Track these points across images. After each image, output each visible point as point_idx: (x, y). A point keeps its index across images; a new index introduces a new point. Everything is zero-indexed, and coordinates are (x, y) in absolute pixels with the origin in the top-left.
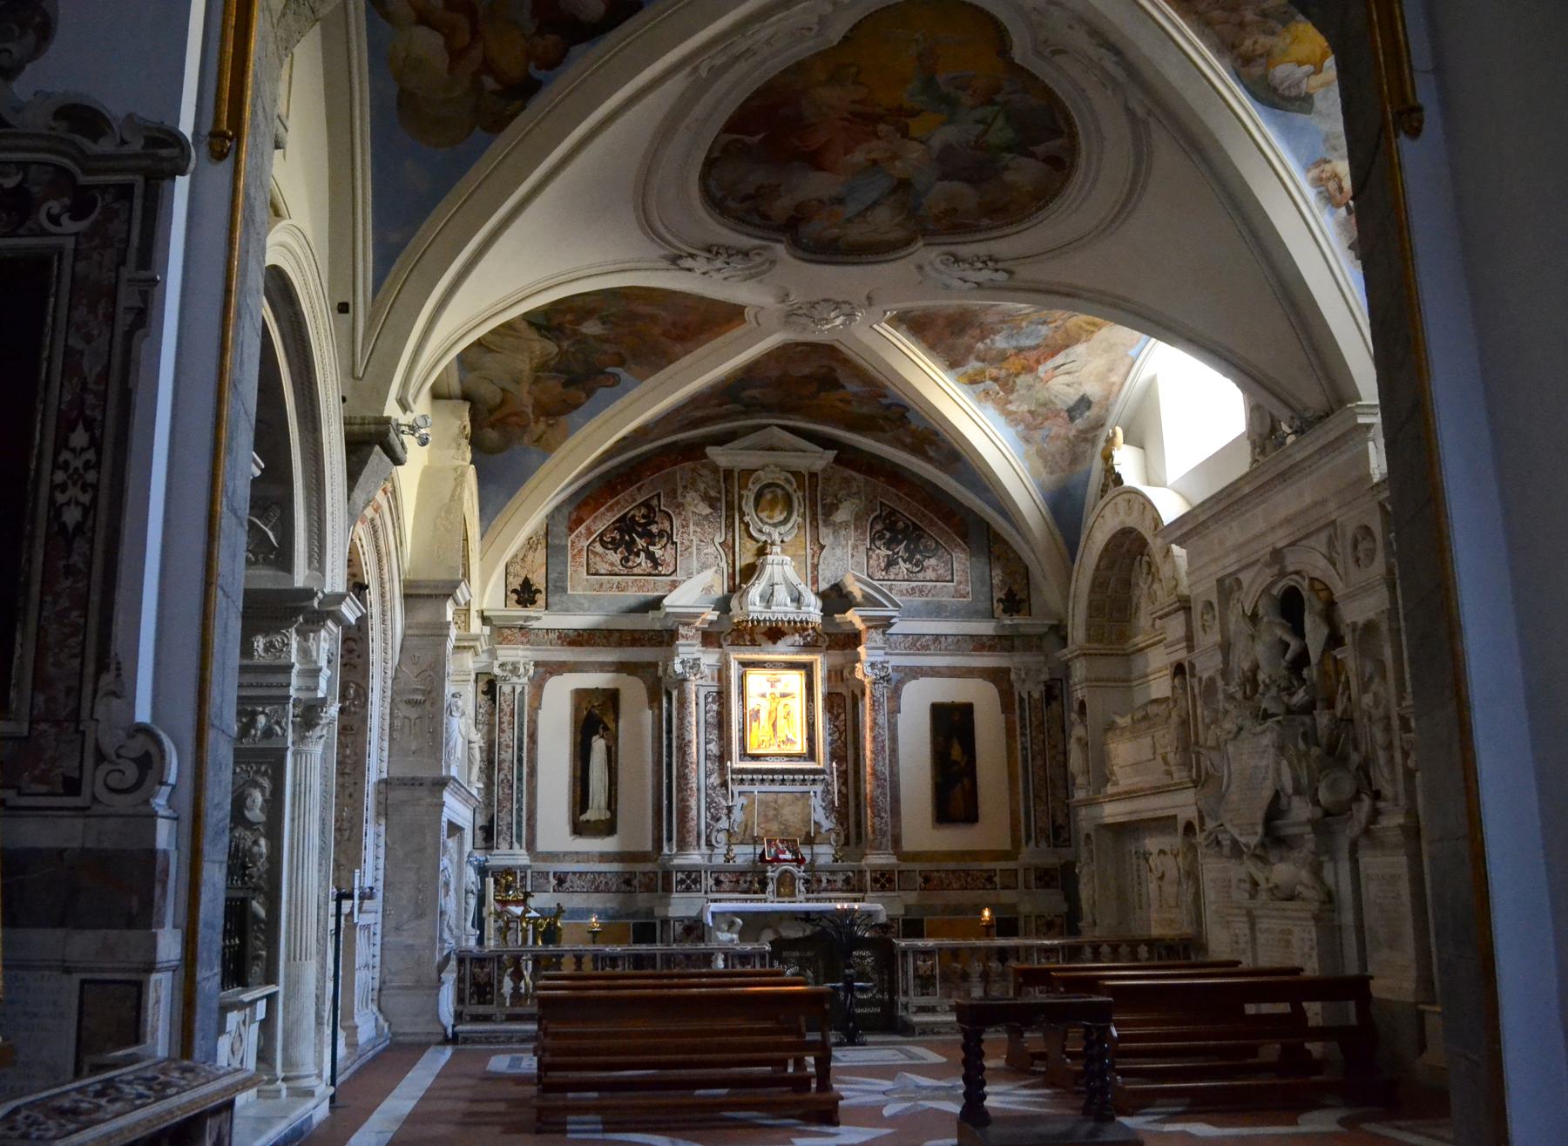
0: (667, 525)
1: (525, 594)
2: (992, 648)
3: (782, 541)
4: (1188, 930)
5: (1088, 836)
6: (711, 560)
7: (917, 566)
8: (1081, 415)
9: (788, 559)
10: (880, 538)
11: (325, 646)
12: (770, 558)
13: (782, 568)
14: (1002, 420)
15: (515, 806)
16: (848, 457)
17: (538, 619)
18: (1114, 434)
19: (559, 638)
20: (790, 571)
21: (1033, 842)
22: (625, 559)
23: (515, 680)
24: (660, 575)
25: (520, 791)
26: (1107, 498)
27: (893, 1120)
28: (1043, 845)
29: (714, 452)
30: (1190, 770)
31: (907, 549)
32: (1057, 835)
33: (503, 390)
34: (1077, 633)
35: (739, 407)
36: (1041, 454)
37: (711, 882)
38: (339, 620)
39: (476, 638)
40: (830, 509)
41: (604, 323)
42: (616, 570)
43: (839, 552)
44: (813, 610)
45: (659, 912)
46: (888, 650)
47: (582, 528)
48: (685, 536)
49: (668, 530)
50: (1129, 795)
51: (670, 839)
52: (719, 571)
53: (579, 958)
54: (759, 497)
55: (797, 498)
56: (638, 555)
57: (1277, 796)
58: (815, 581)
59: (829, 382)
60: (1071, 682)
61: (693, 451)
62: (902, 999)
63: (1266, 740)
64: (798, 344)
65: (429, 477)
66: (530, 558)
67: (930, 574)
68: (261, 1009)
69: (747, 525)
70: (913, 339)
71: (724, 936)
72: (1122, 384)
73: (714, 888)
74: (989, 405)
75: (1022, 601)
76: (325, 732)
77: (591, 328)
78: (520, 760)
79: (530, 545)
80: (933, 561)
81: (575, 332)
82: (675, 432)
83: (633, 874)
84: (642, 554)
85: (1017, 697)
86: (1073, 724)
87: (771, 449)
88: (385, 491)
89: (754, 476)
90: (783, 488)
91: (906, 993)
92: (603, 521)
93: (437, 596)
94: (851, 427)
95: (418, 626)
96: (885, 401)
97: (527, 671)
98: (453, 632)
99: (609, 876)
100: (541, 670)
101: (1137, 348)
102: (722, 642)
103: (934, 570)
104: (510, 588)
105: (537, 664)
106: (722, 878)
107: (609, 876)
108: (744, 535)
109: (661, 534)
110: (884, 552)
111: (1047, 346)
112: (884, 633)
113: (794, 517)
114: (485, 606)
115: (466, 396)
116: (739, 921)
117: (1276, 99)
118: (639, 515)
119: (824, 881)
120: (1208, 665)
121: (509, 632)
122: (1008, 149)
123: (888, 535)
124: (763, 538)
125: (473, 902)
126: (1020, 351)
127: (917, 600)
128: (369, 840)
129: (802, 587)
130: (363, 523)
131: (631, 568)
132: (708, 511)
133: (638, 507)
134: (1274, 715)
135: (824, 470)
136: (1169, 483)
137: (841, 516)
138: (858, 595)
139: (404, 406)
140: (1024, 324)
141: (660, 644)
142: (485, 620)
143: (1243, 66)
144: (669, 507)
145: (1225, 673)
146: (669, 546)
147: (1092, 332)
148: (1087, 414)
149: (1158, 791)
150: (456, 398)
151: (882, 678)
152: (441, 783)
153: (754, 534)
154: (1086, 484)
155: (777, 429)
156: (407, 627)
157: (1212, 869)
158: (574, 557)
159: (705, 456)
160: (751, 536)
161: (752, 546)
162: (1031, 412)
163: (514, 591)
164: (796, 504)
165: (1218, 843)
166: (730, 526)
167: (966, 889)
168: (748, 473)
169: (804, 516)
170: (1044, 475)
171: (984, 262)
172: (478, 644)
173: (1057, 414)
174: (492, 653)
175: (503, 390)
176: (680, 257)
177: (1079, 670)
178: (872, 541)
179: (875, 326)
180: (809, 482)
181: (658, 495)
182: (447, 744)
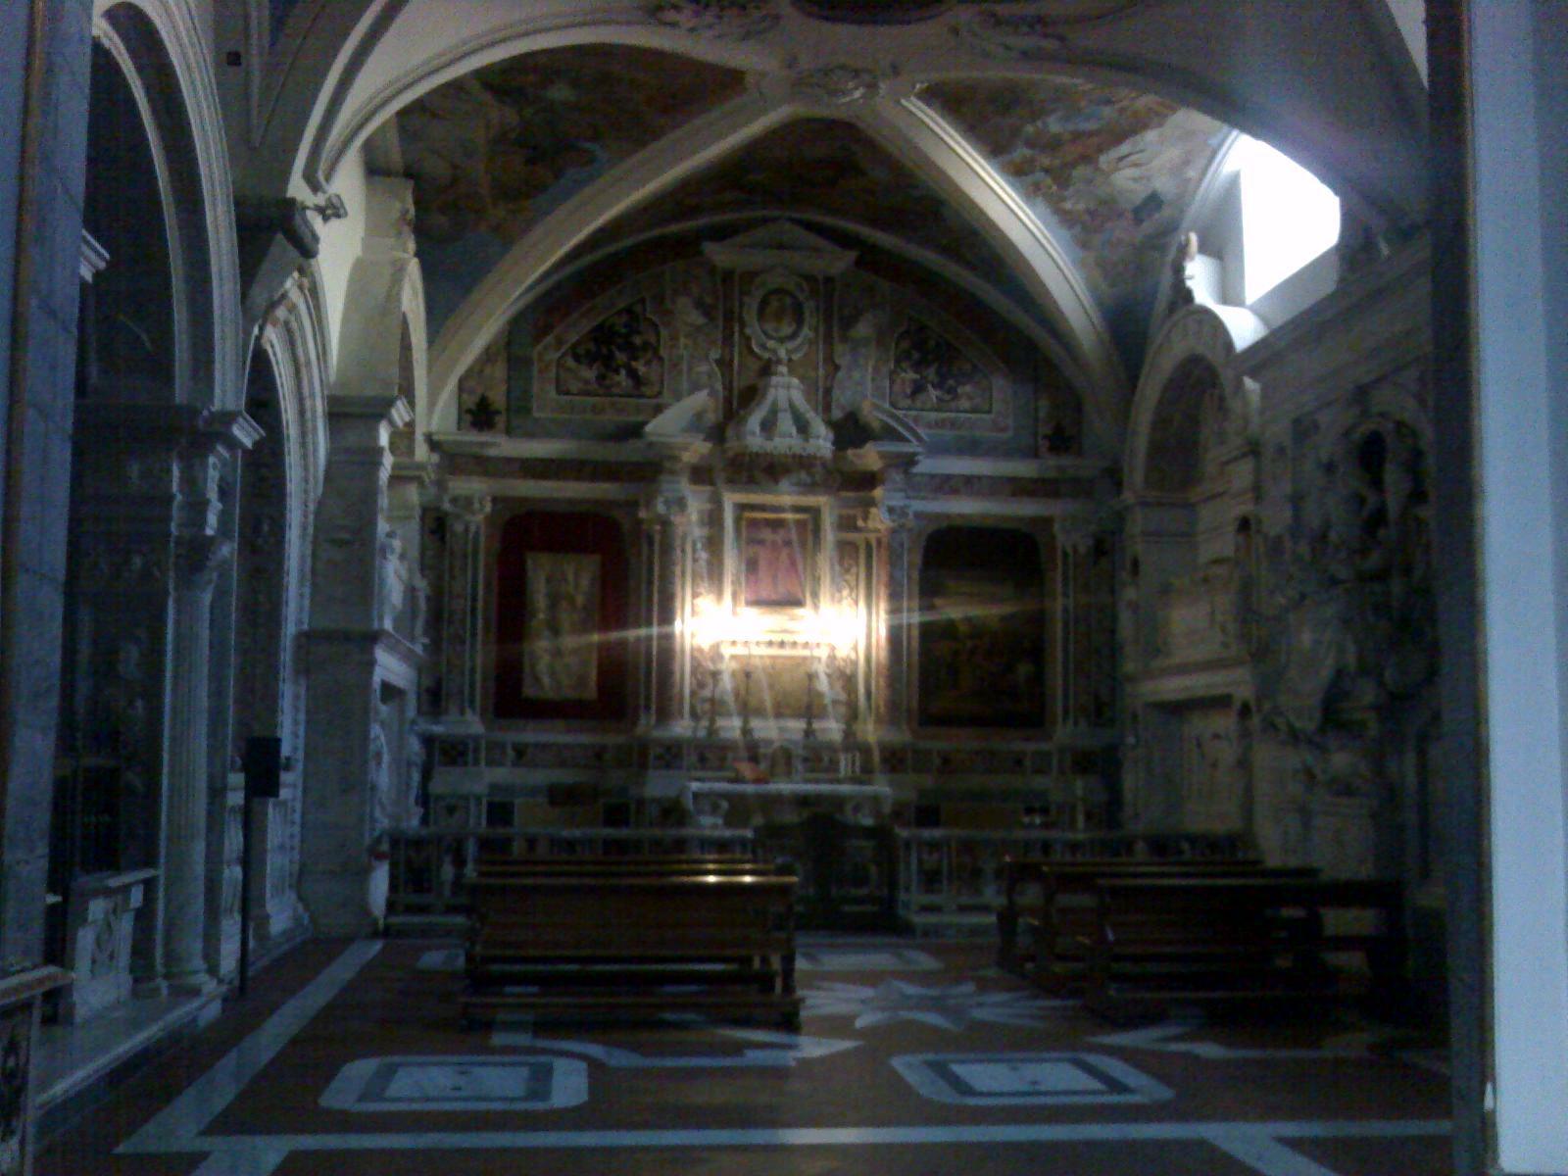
1: (480, 415)
3: (790, 360)
5: (1135, 716)
6: (704, 379)
7: (949, 392)
9: (795, 381)
11: (213, 475)
12: (775, 380)
13: (786, 390)
14: (1054, 219)
16: (871, 259)
17: (493, 444)
20: (798, 397)
21: (1071, 721)
22: (601, 378)
23: (469, 517)
24: (642, 396)
26: (1176, 317)
27: (861, 1034)
31: (938, 373)
32: (1099, 712)
33: (455, 167)
34: (1136, 474)
37: (694, 758)
38: (233, 444)
39: (421, 467)
40: (848, 323)
43: (856, 375)
44: (822, 442)
47: (549, 339)
50: (1183, 669)
51: (647, 708)
52: (712, 393)
53: (532, 842)
54: (764, 304)
55: (809, 307)
56: (617, 371)
57: (1340, 673)
58: (827, 408)
61: (685, 247)
62: (902, 896)
63: (1329, 611)
64: (809, 121)
65: (361, 273)
66: (488, 371)
67: (965, 404)
68: (137, 897)
69: (748, 339)
71: (707, 820)
72: (1201, 180)
76: (215, 576)
77: (560, 93)
78: (474, 610)
79: (488, 356)
80: (968, 388)
84: (623, 372)
85: (1059, 553)
87: (781, 247)
88: (301, 287)
90: (793, 296)
91: (907, 889)
92: (577, 329)
94: (875, 223)
95: (347, 451)
97: (482, 506)
98: (388, 460)
101: (1220, 136)
104: (465, 407)
106: (708, 755)
110: (911, 375)
112: (906, 472)
113: (806, 331)
114: (434, 428)
115: (410, 173)
118: (620, 324)
120: (1276, 519)
123: (916, 355)
124: (766, 355)
125: (416, 776)
126: (1077, 136)
127: (948, 434)
128: (286, 703)
129: (810, 415)
130: (274, 325)
132: (700, 320)
133: (619, 313)
134: (1343, 582)
137: (863, 329)
138: (875, 425)
139: (316, 188)
140: (1083, 104)
142: (434, 445)
145: (1296, 528)
146: (655, 362)
147: (1166, 116)
150: (397, 175)
152: (373, 638)
153: (756, 349)
155: (787, 226)
156: (332, 453)
157: (1267, 755)
158: (540, 372)
159: (700, 253)
160: (751, 351)
161: (754, 366)
162: (1089, 212)
163: (469, 411)
164: (807, 314)
165: (1273, 726)
166: (727, 341)
168: (751, 276)
169: (816, 330)
171: (1031, 26)
172: (424, 474)
173: (1120, 215)
175: (455, 167)
176: (660, 8)
177: (1138, 523)
178: (898, 362)
180: (823, 288)
181: (643, 301)
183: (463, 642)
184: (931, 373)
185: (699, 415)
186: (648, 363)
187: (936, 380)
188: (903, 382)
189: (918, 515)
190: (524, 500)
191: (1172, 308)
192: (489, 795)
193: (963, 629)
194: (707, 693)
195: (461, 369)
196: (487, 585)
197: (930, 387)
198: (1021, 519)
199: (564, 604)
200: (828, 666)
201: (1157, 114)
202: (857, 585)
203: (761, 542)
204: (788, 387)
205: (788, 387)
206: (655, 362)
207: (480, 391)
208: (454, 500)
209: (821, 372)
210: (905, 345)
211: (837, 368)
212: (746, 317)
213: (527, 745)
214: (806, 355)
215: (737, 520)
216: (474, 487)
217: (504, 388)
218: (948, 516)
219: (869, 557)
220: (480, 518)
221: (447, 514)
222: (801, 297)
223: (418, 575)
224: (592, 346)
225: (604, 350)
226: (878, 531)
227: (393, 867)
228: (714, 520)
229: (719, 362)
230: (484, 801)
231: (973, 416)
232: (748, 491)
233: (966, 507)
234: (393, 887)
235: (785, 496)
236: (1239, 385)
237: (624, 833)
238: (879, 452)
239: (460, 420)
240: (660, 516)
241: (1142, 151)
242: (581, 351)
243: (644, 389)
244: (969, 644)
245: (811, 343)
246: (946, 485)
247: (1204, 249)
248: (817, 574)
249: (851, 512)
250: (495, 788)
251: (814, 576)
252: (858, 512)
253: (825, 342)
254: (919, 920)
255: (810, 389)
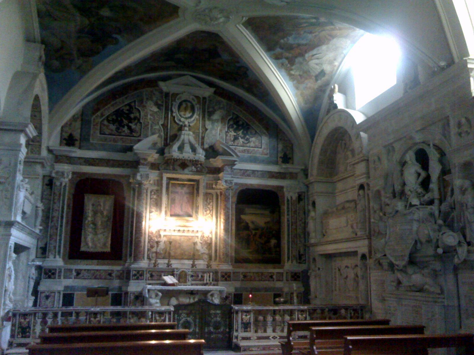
0: (138, 115)
1: (69, 141)
2: (277, 178)
3: (189, 126)
4: (362, 302)
5: (314, 259)
8: (321, 79)
9: (191, 133)
10: (233, 127)
12: (183, 132)
13: (187, 136)
15: (58, 238)
16: (220, 92)
17: (75, 152)
18: (334, 87)
19: (85, 162)
22: (118, 129)
23: (62, 179)
24: (133, 136)
25: (61, 230)
28: (295, 262)
29: (161, 84)
30: (365, 231)
31: (243, 133)
34: (314, 171)
35: (173, 63)
36: (302, 94)
37: (148, 275)
40: (211, 114)
42: (113, 133)
43: (214, 132)
44: (201, 155)
45: (124, 289)
46: (232, 176)
47: (99, 113)
48: (146, 120)
49: (138, 117)
50: (335, 242)
51: (131, 255)
52: (160, 136)
55: (197, 107)
56: (124, 127)
58: (203, 144)
59: (213, 53)
60: (310, 193)
61: (152, 83)
62: (235, 334)
67: (252, 144)
69: (174, 117)
72: (339, 66)
73: (150, 278)
74: (283, 70)
75: (290, 158)
78: (62, 217)
79: (74, 118)
80: (253, 139)
82: (142, 73)
83: (112, 270)
84: (126, 127)
85: (286, 198)
86: (309, 211)
87: (187, 85)
89: (178, 97)
90: (191, 103)
91: (237, 331)
93: (15, 130)
94: (223, 78)
96: (238, 65)
97: (68, 175)
99: (102, 271)
100: (75, 176)
102: (160, 168)
103: (254, 143)
104: (63, 138)
105: (74, 173)
106: (154, 274)
107: (102, 271)
108: (173, 122)
109: (135, 118)
110: (233, 133)
112: (232, 168)
113: (196, 116)
116: (160, 294)
119: (200, 276)
121: (61, 158)
123: (235, 126)
124: (181, 123)
127: (246, 155)
129: (196, 146)
131: (120, 132)
133: (126, 105)
135: (209, 97)
136: (357, 109)
137: (216, 116)
138: (221, 150)
140: (302, 32)
141: (131, 167)
142: (50, 151)
144: (139, 106)
146: (138, 124)
148: (323, 79)
149: (348, 240)
151: (230, 187)
153: (177, 121)
154: (319, 110)
157: (375, 275)
159: (157, 86)
161: (176, 127)
163: (65, 139)
165: (380, 264)
166: (166, 118)
167: (261, 281)
168: (175, 95)
170: (303, 104)
174: (52, 166)
178: (228, 128)
179: (237, 25)
180: (203, 101)
181: (135, 102)
182: (16, 205)
183: (57, 229)
184: (240, 133)
185: (155, 144)
186: (136, 124)
187: (242, 136)
188: (230, 135)
189: (236, 184)
190: (84, 174)
191: (328, 111)
192: (64, 290)
193: (251, 226)
194: (154, 250)
195: (62, 124)
196: (68, 206)
197: (240, 138)
198: (273, 186)
199: (99, 215)
200: (201, 240)
202: (212, 210)
203: (177, 193)
204: (189, 135)
205: (189, 135)
206: (138, 124)
207: (70, 131)
208: (57, 173)
209: (201, 131)
210: (231, 123)
211: (206, 130)
212: (174, 110)
213: (81, 270)
214: (195, 124)
215: (168, 184)
216: (66, 168)
217: (79, 131)
218: (246, 185)
219: (217, 198)
220: (67, 180)
221: (53, 178)
222: (194, 103)
223: (39, 202)
224: (114, 117)
225: (119, 119)
226: (221, 189)
227: (13, 325)
228: (159, 183)
229: (163, 125)
230: (62, 293)
231: (256, 149)
232: (173, 173)
233: (254, 182)
234: (12, 336)
235: (186, 175)
236: (358, 136)
237: (119, 308)
238: (222, 160)
239: (61, 142)
240: (137, 180)
241: (319, 54)
242: (110, 119)
243: (134, 134)
244: (254, 232)
245: (198, 120)
246: (245, 173)
247: (340, 91)
248: (198, 205)
249: (211, 182)
250: (66, 287)
251: (196, 206)
252: (214, 182)
253: (202, 118)
254: (243, 343)
255: (196, 134)
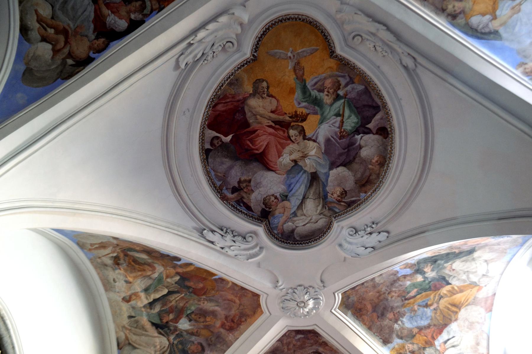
41: (190, 320)
70: (357, 322)
81: (176, 328)
111: (435, 325)
117: (479, 35)
122: (357, 131)
143: (453, 20)
201: (453, 312)
